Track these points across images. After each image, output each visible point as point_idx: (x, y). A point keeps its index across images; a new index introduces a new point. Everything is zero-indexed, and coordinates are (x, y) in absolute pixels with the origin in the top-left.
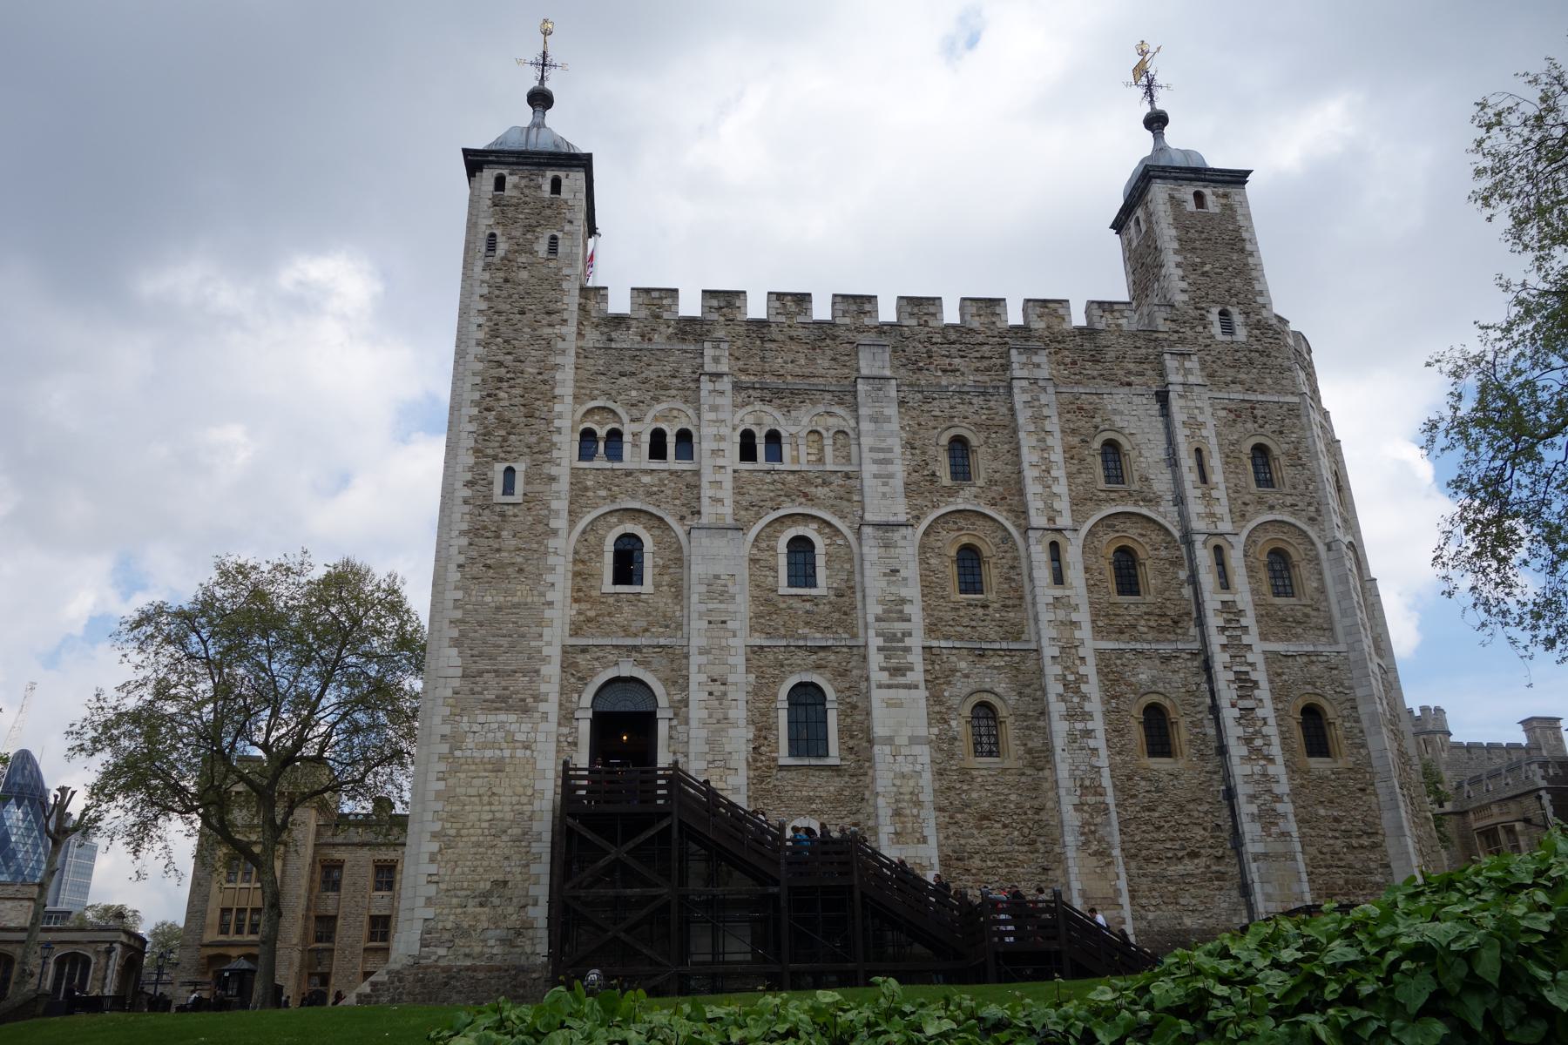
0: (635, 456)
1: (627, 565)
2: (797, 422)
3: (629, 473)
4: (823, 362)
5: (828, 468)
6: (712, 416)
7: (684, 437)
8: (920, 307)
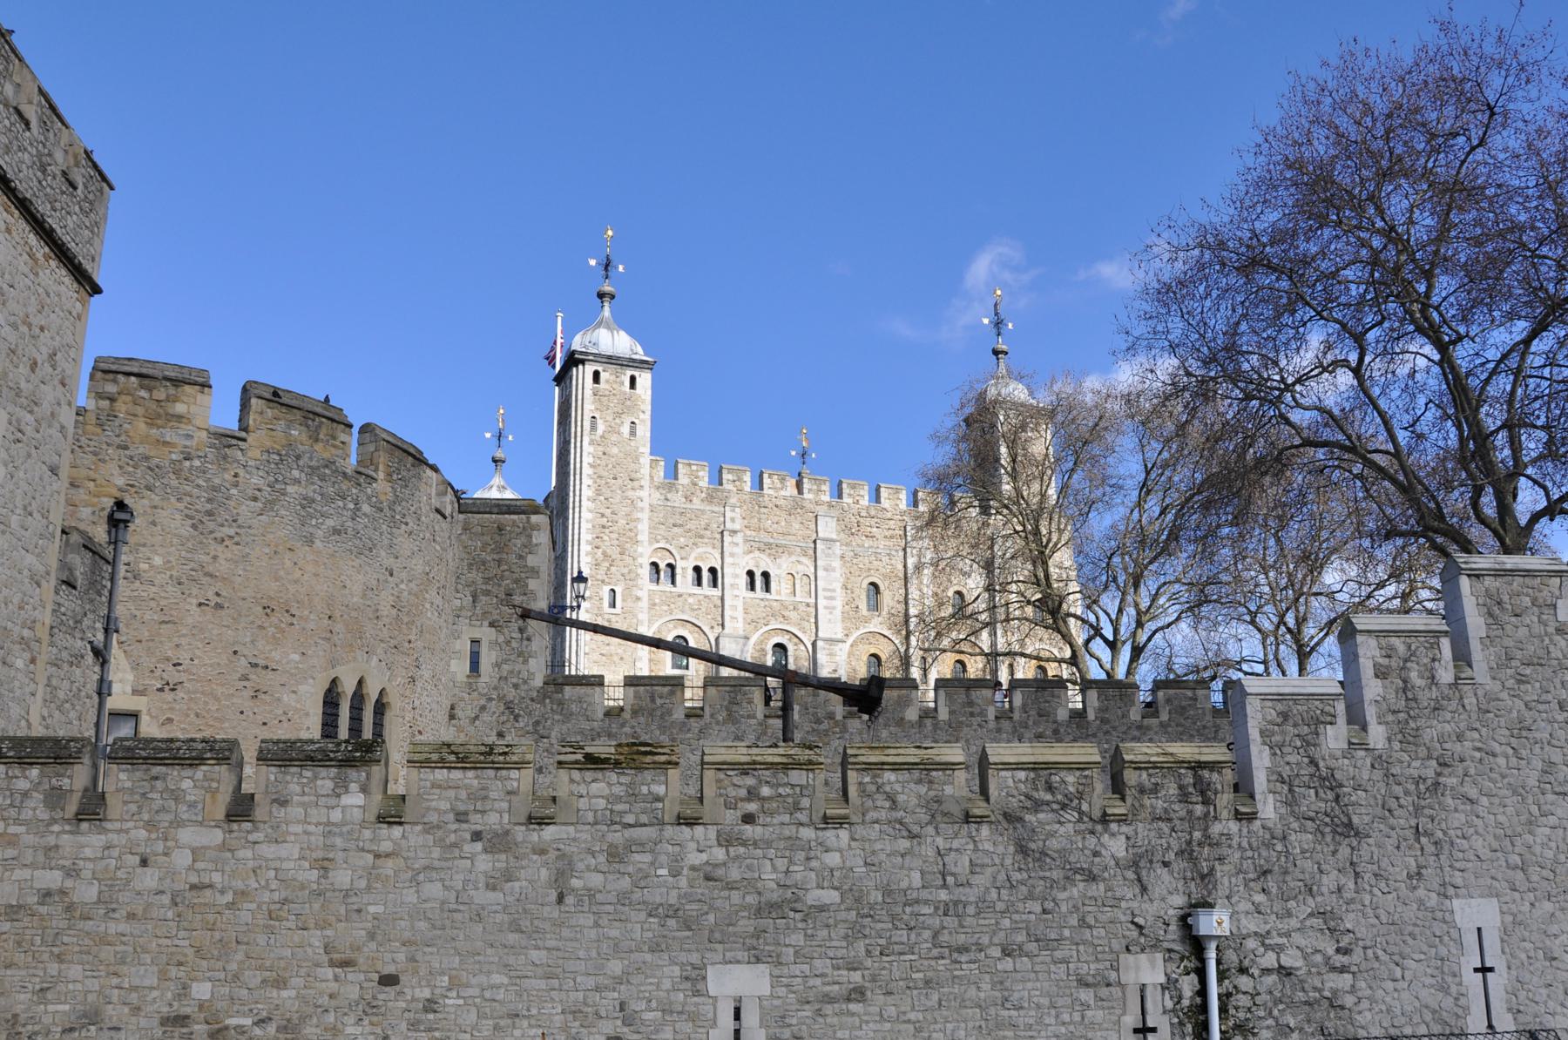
2: (779, 567)
3: (680, 596)
5: (798, 599)
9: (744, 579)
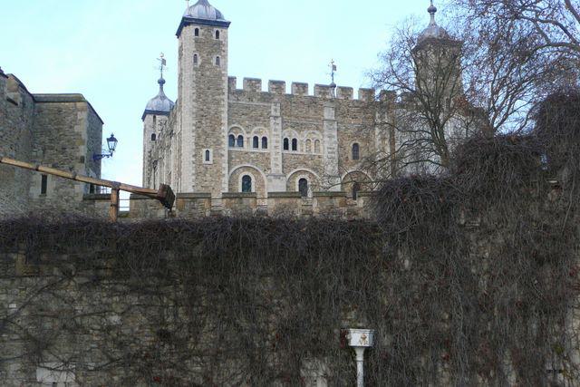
0: (248, 146)
3: (246, 153)
4: (312, 112)
6: (274, 133)
7: (265, 139)
9: (281, 145)
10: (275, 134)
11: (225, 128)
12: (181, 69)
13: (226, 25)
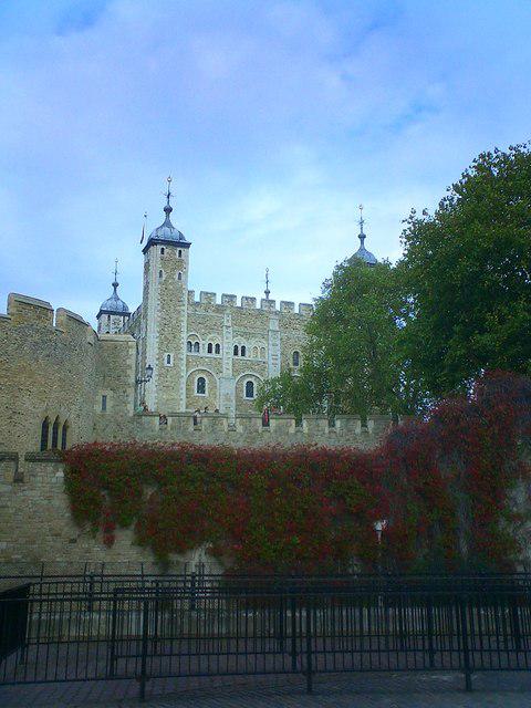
1: (201, 389)
7: (218, 346)
8: (289, 304)
10: (228, 342)
11: (184, 335)
12: (147, 283)
13: (187, 245)
